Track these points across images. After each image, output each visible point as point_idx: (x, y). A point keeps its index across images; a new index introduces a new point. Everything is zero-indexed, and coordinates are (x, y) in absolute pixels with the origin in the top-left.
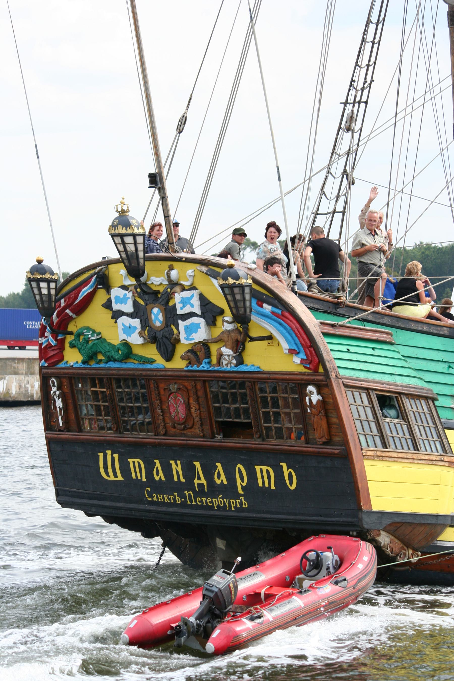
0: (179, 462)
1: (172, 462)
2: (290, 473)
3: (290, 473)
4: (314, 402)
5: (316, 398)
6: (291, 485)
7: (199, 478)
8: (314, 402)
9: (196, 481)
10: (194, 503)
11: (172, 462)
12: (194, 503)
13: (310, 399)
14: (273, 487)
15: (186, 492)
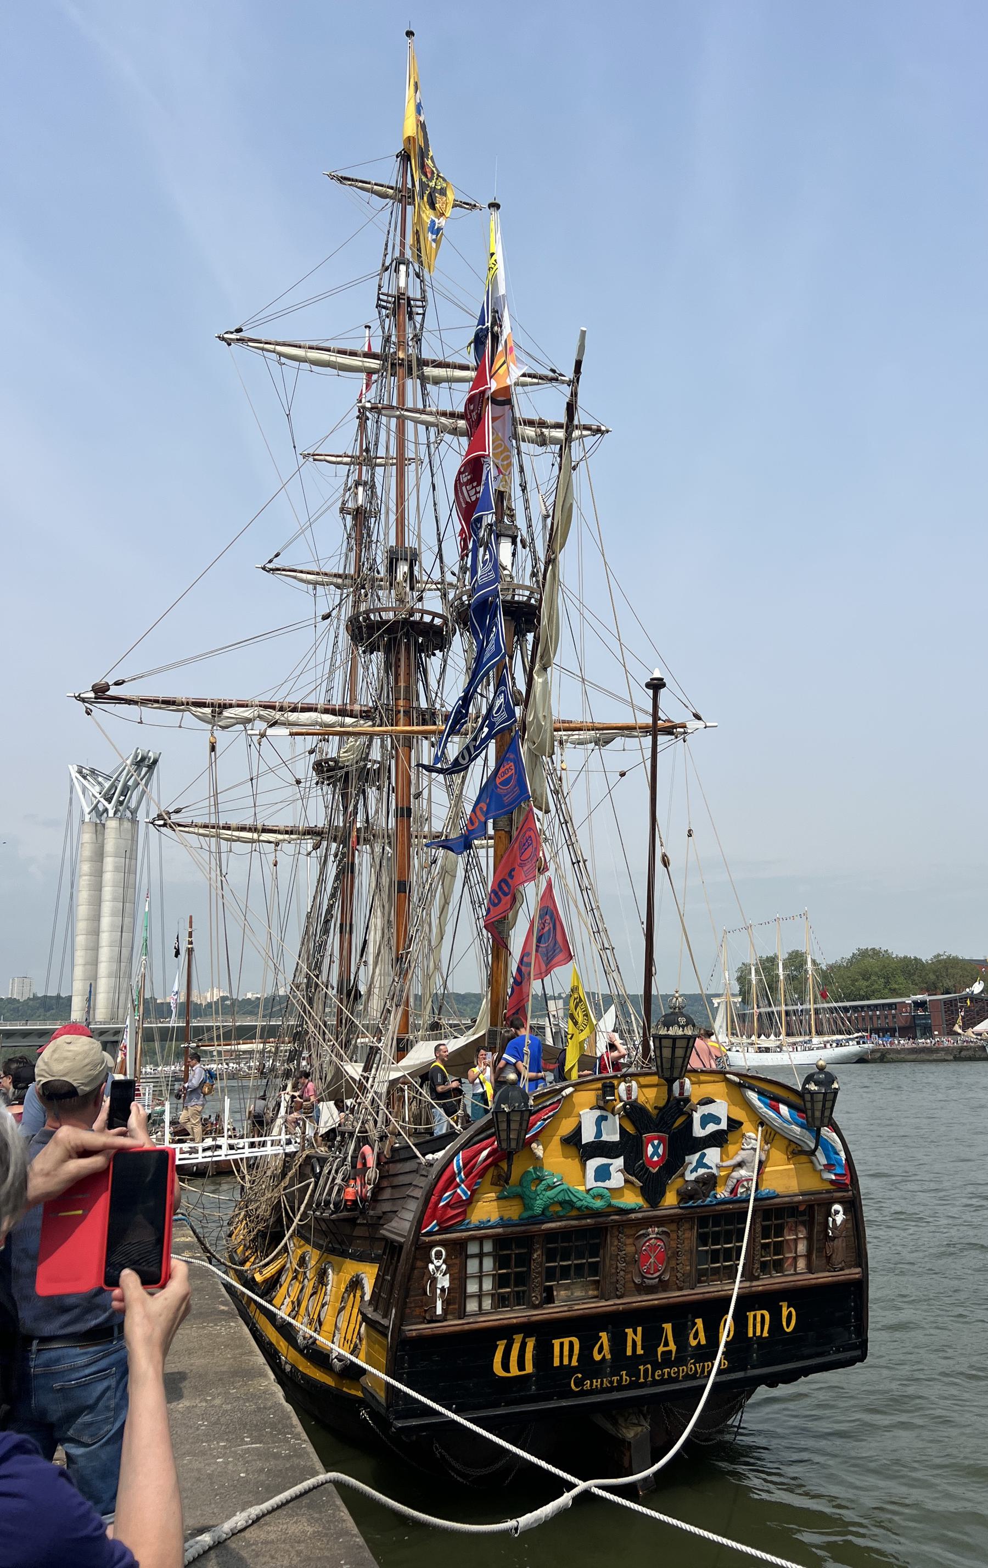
0: (639, 1329)
1: (629, 1331)
2: (790, 1313)
3: (790, 1313)
4: (839, 1222)
5: (840, 1218)
6: (788, 1327)
7: (666, 1344)
8: (839, 1222)
9: (661, 1349)
10: (650, 1379)
11: (629, 1331)
12: (650, 1379)
13: (834, 1220)
14: (765, 1334)
15: (641, 1367)
